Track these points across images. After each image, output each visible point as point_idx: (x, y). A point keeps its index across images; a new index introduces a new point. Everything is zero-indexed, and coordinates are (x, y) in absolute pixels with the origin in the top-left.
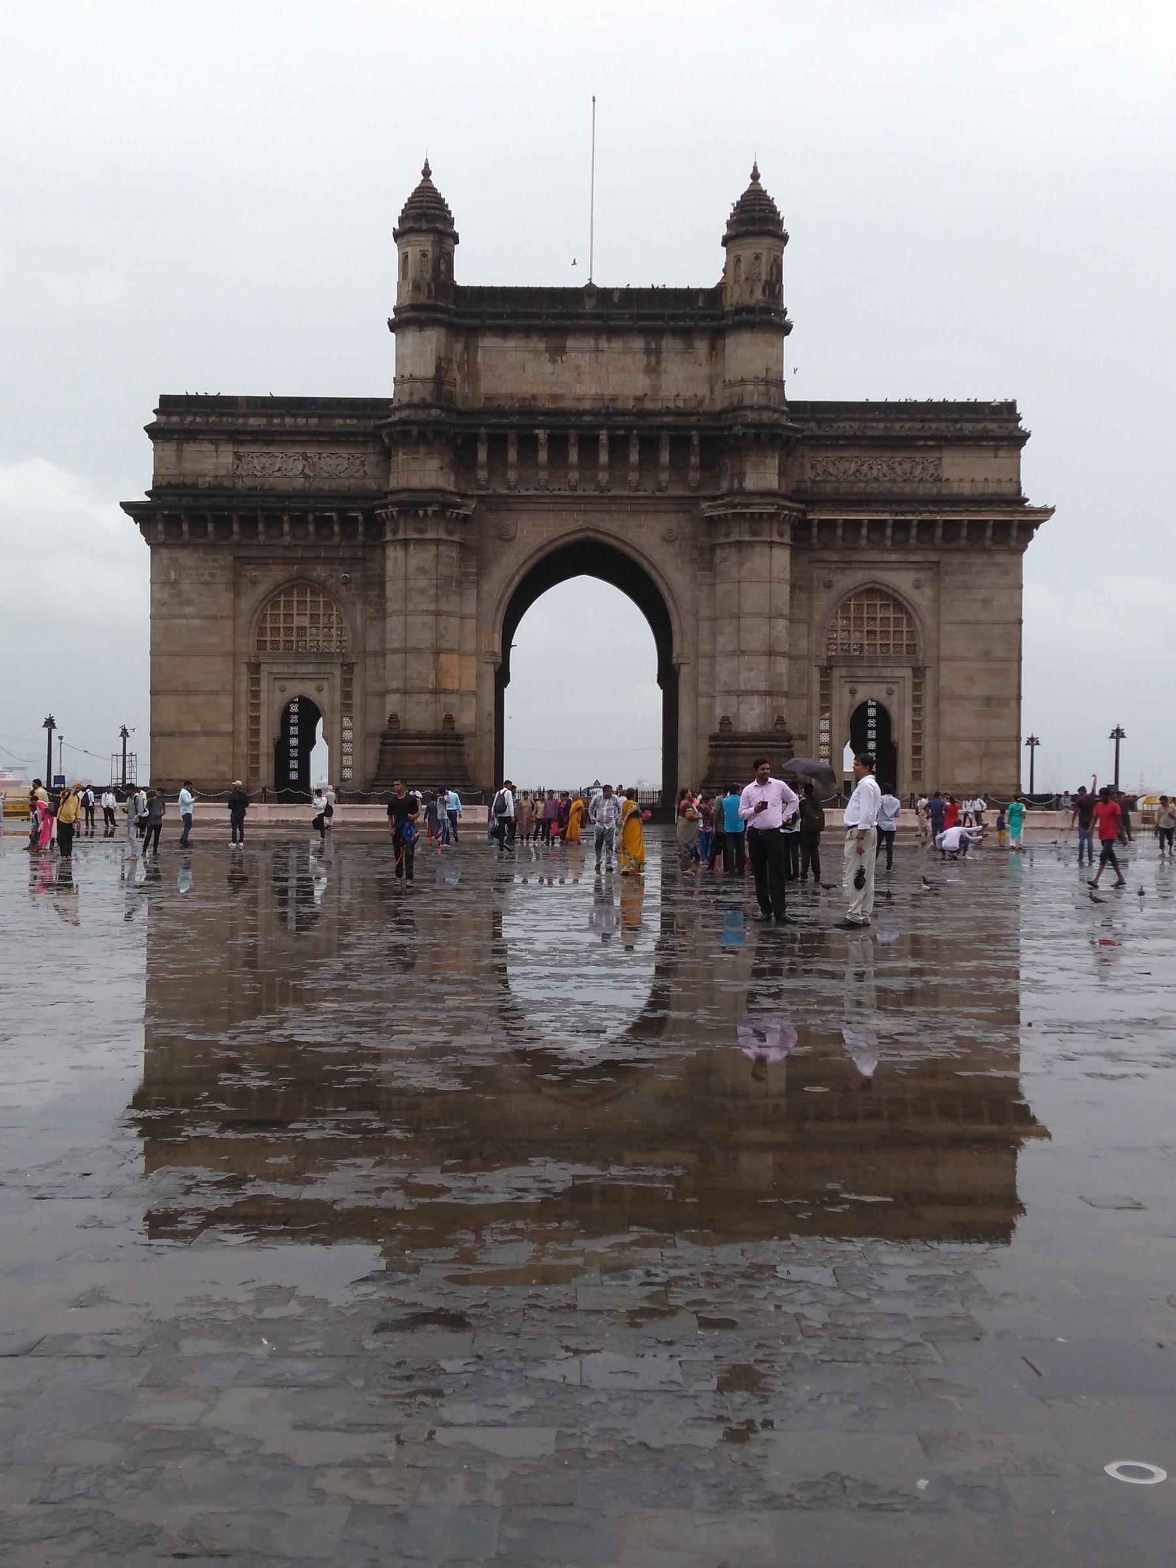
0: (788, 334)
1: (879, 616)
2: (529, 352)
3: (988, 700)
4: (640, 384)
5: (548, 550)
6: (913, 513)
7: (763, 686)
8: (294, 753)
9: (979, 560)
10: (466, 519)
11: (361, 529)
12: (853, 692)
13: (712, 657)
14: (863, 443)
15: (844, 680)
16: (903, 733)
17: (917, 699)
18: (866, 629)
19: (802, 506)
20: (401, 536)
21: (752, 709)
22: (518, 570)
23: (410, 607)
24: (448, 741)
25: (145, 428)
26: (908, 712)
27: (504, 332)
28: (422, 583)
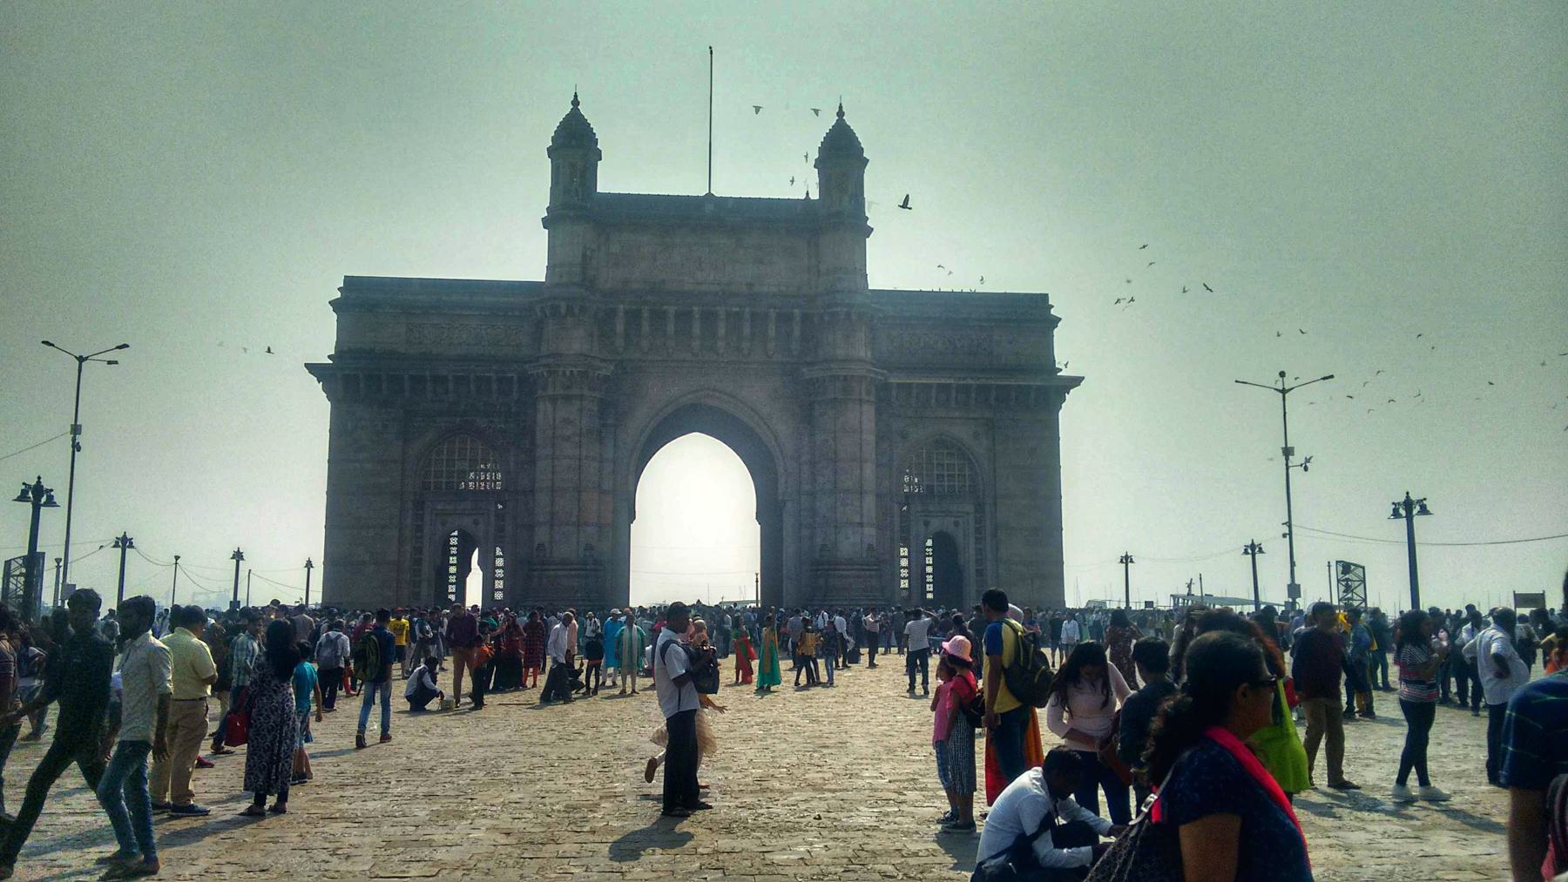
0: (868, 237)
1: (946, 462)
6: (972, 379)
7: (857, 519)
8: (452, 579)
11: (515, 387)
12: (926, 524)
13: (812, 494)
15: (918, 514)
17: (978, 530)
18: (935, 472)
19: (885, 371)
20: (550, 392)
21: (848, 538)
23: (558, 453)
24: (588, 567)
26: (972, 540)
28: (569, 431)
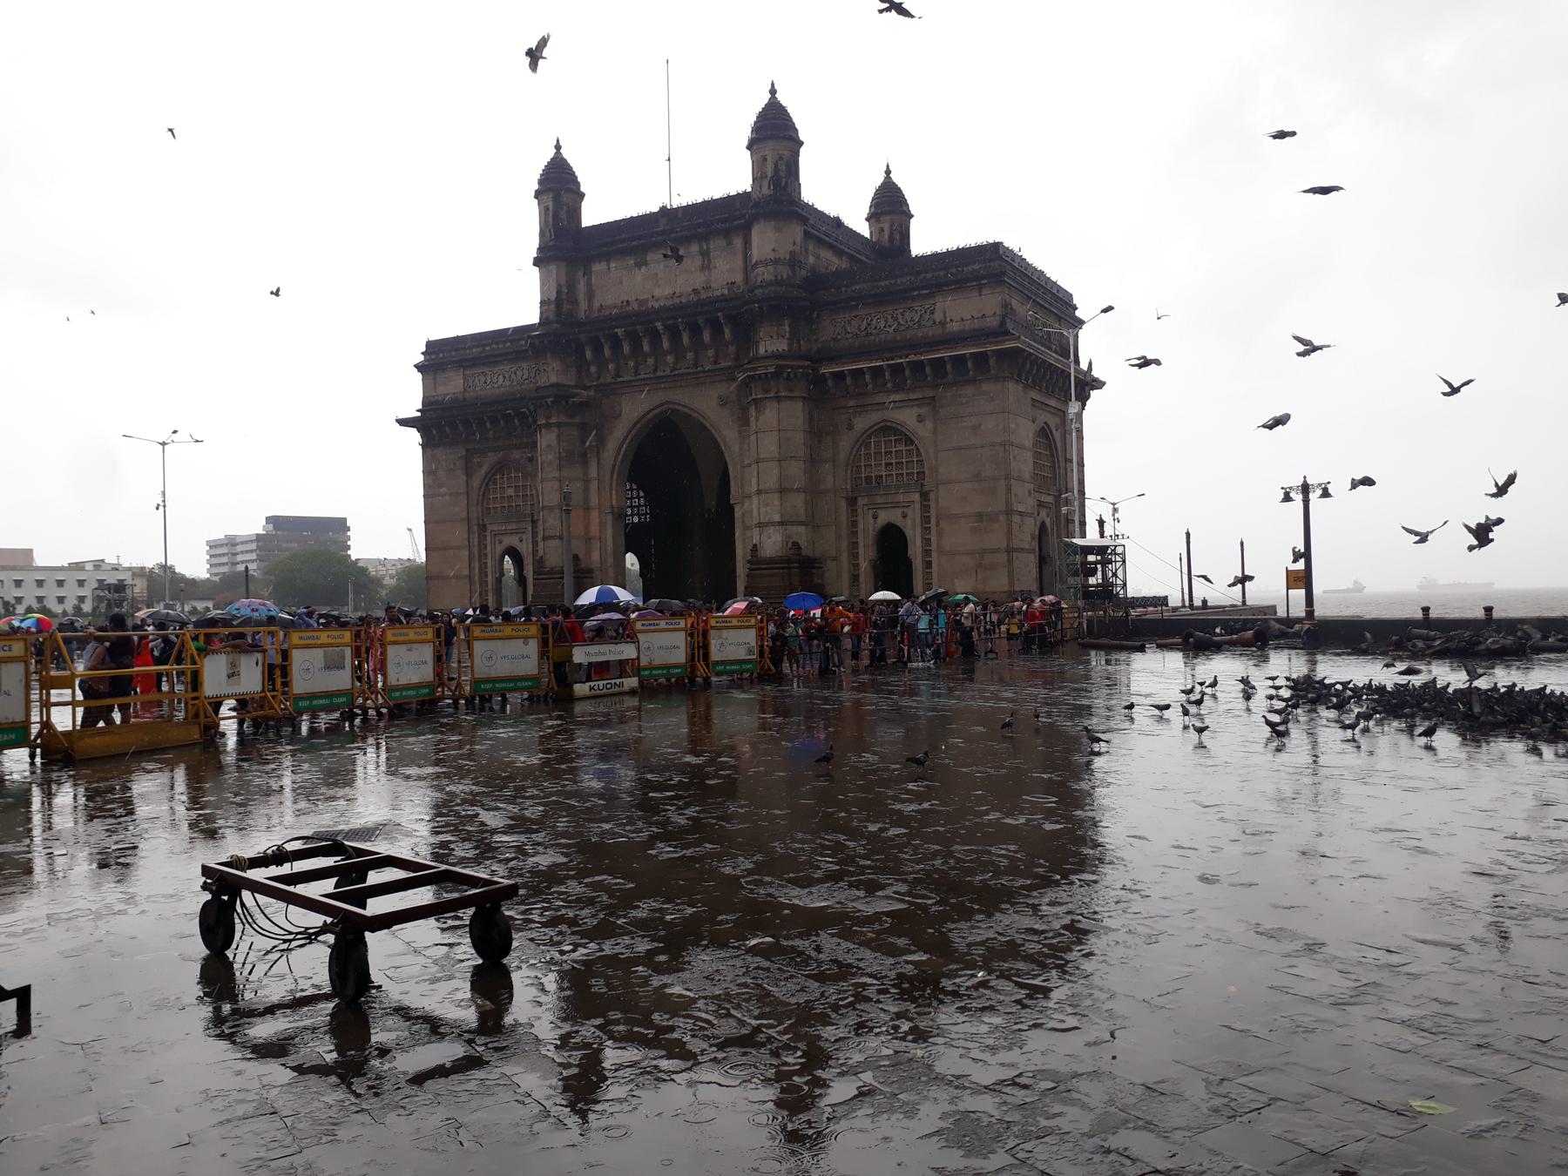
1: (894, 450)
2: (624, 269)
3: (980, 516)
4: (698, 280)
5: (645, 420)
7: (777, 518)
9: (968, 390)
10: (584, 405)
12: (875, 517)
14: (870, 301)
15: (866, 508)
16: (915, 551)
17: (926, 520)
21: (769, 538)
22: (625, 439)
25: (415, 366)
26: (919, 530)
27: (607, 257)
